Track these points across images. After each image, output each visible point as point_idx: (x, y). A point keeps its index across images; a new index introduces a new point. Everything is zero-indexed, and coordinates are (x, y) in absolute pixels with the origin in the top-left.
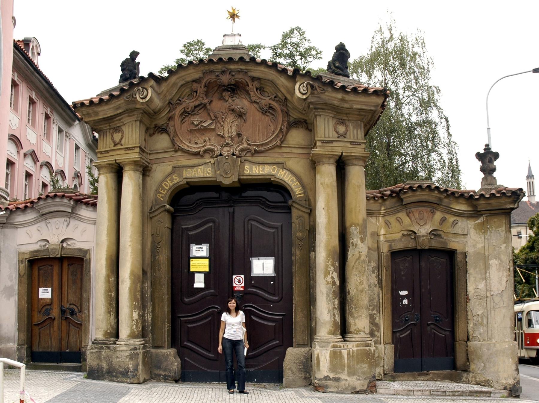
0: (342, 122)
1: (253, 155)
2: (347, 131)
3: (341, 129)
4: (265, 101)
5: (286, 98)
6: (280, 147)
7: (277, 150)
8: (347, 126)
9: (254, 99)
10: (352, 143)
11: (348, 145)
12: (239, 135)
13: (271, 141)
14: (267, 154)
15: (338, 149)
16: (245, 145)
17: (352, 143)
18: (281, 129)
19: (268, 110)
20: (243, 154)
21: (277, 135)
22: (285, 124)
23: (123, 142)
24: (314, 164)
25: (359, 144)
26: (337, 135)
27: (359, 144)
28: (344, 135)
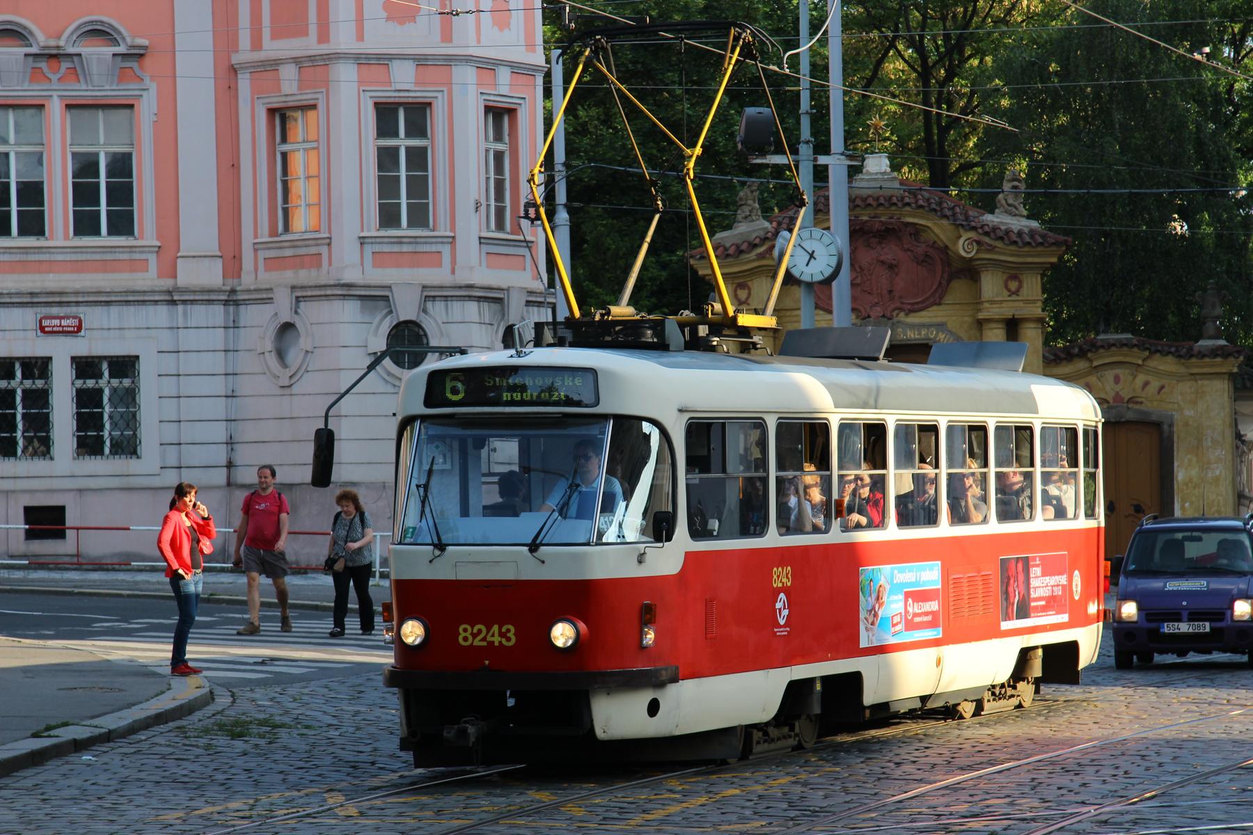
0: (1014, 277)
1: (907, 315)
2: (1020, 287)
3: (1013, 285)
4: (921, 249)
5: (946, 247)
6: (940, 304)
7: (935, 308)
8: (1021, 282)
9: (906, 246)
10: (1027, 302)
11: (1021, 304)
12: (890, 292)
13: (927, 299)
14: (922, 313)
15: (1007, 311)
16: (898, 305)
17: (1027, 302)
18: (940, 283)
19: (924, 261)
20: (895, 314)
21: (936, 291)
22: (945, 276)
23: (750, 301)
24: (980, 324)
25: (1034, 301)
26: (1006, 293)
27: (1034, 301)
28: (1016, 293)
